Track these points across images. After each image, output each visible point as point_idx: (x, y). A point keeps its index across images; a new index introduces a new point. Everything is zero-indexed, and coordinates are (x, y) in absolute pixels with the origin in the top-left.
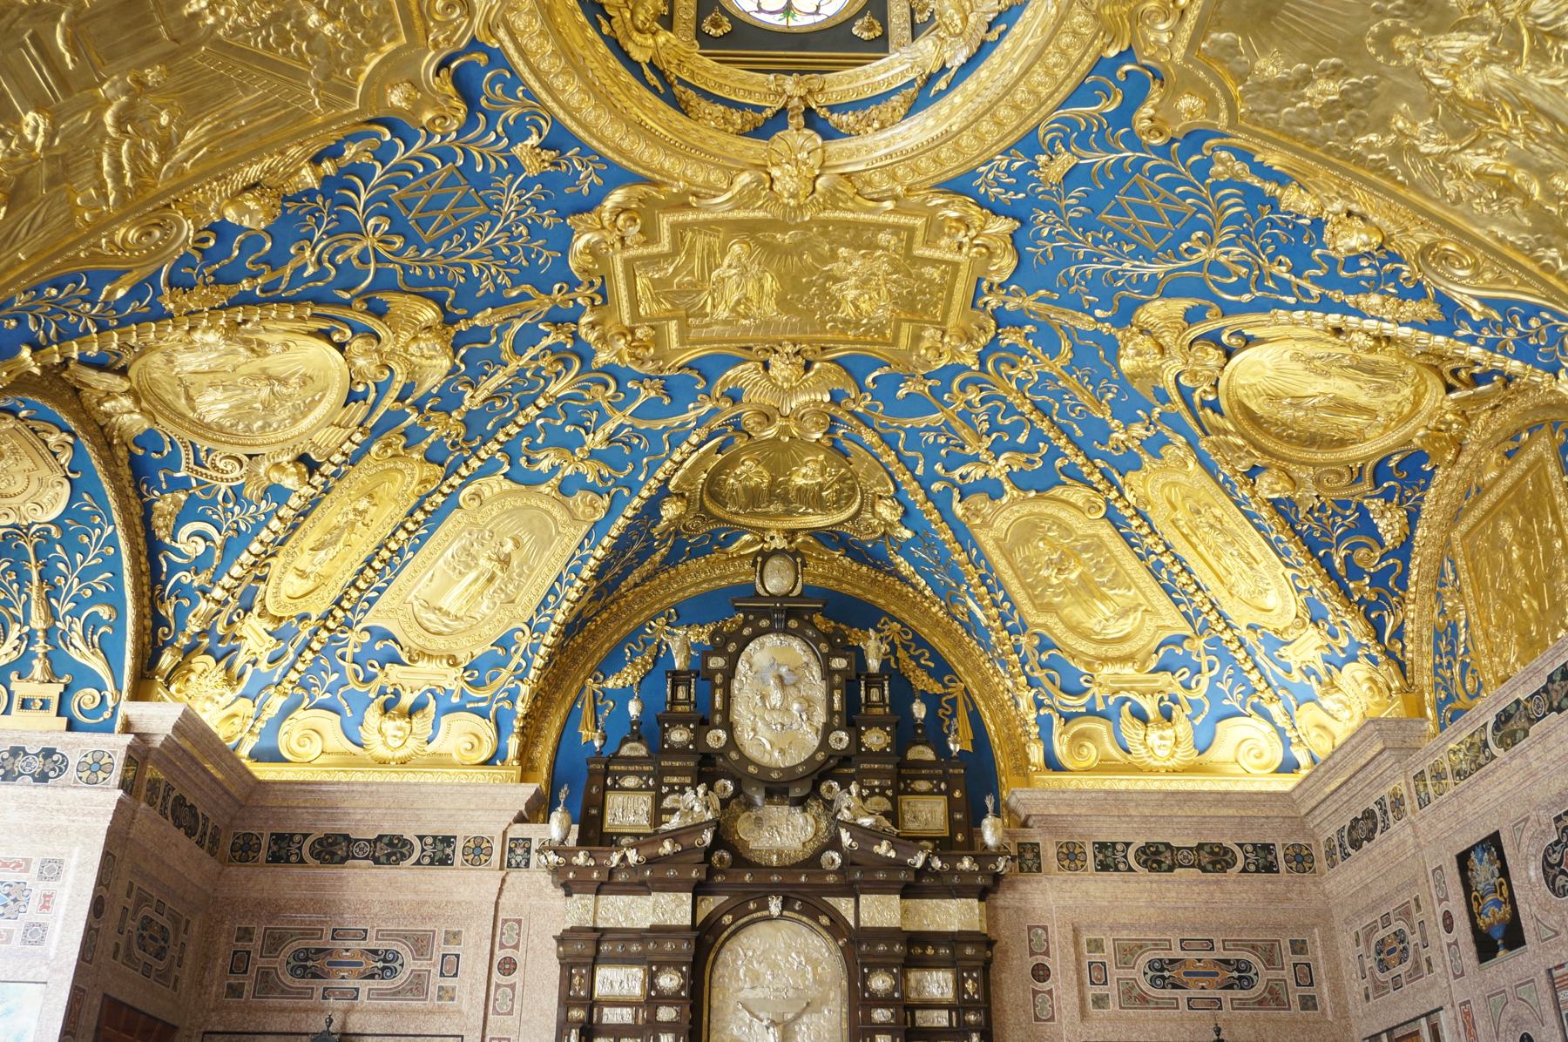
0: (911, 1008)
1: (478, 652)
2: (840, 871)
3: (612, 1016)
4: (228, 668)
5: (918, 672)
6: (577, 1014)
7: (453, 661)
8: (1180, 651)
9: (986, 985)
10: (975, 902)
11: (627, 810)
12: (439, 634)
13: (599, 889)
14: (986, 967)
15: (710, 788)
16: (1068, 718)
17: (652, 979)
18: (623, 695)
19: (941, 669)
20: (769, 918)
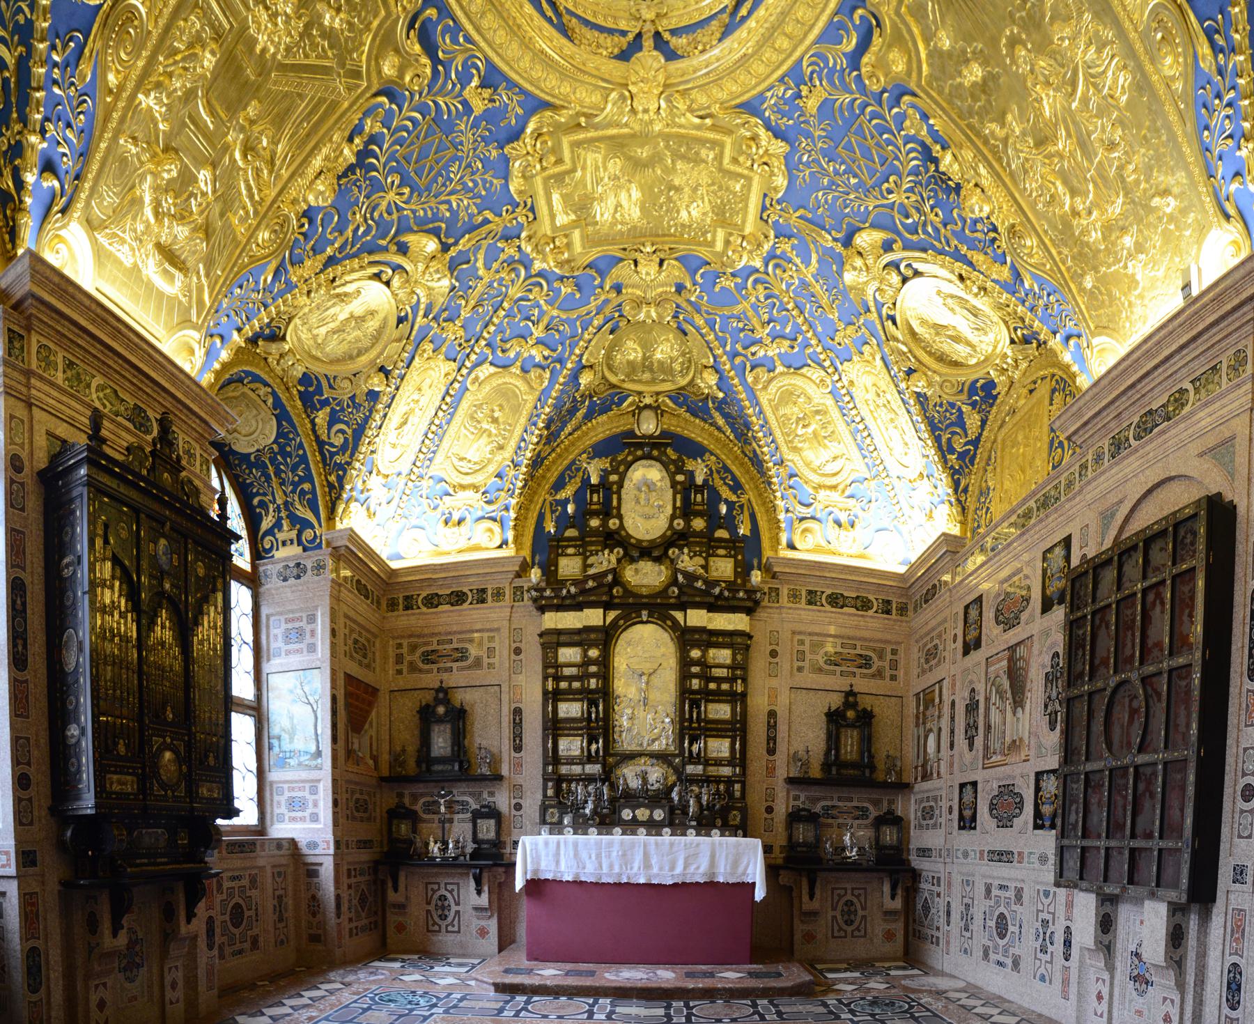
0: (711, 667)
1: (489, 482)
2: (678, 597)
3: (567, 671)
4: (368, 509)
5: (724, 487)
6: (551, 671)
7: (475, 488)
8: (861, 487)
9: (746, 658)
10: (743, 616)
11: (569, 566)
12: (467, 474)
13: (559, 608)
14: (748, 647)
15: (611, 551)
16: (802, 519)
17: (585, 652)
18: (565, 503)
19: (736, 487)
20: (642, 622)
